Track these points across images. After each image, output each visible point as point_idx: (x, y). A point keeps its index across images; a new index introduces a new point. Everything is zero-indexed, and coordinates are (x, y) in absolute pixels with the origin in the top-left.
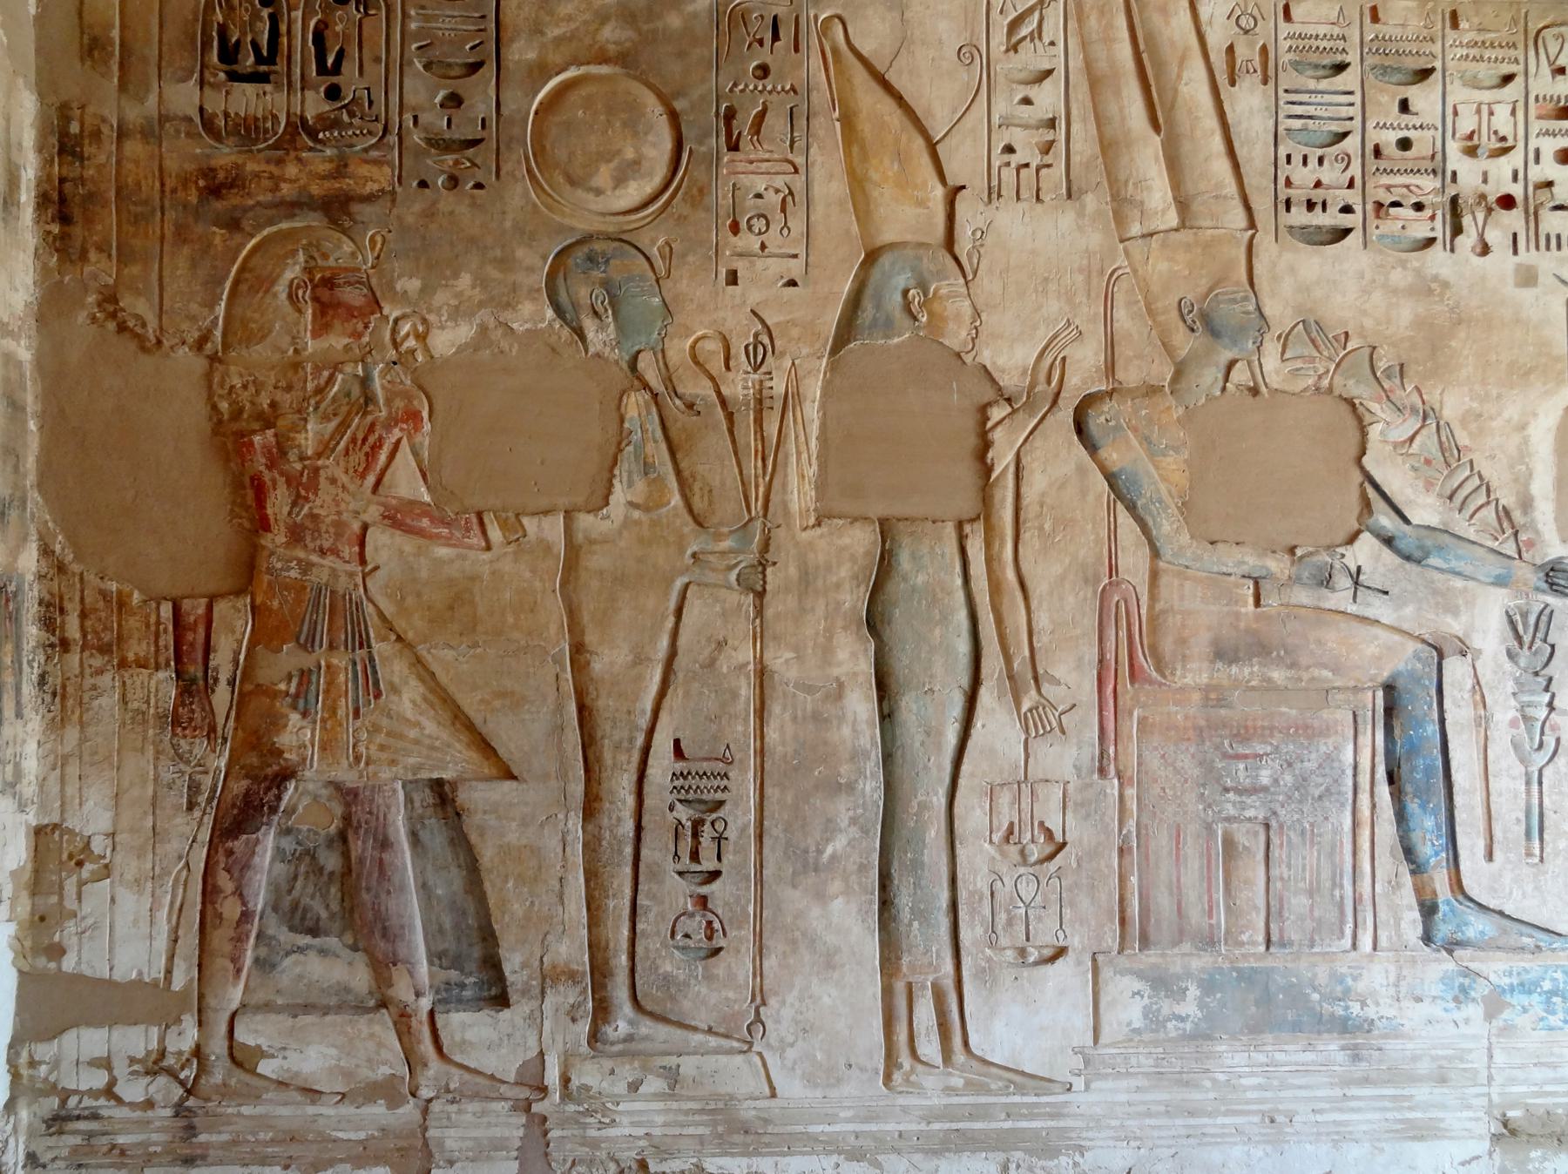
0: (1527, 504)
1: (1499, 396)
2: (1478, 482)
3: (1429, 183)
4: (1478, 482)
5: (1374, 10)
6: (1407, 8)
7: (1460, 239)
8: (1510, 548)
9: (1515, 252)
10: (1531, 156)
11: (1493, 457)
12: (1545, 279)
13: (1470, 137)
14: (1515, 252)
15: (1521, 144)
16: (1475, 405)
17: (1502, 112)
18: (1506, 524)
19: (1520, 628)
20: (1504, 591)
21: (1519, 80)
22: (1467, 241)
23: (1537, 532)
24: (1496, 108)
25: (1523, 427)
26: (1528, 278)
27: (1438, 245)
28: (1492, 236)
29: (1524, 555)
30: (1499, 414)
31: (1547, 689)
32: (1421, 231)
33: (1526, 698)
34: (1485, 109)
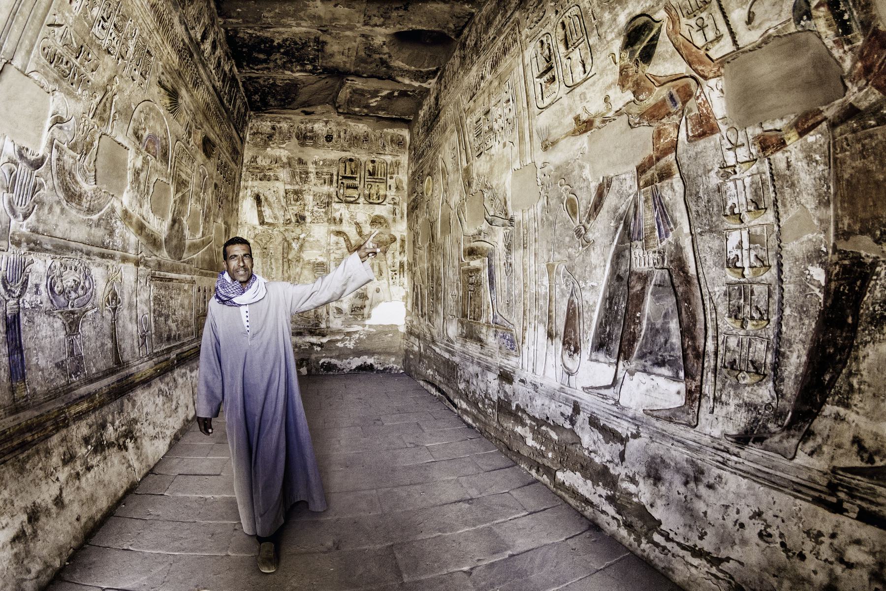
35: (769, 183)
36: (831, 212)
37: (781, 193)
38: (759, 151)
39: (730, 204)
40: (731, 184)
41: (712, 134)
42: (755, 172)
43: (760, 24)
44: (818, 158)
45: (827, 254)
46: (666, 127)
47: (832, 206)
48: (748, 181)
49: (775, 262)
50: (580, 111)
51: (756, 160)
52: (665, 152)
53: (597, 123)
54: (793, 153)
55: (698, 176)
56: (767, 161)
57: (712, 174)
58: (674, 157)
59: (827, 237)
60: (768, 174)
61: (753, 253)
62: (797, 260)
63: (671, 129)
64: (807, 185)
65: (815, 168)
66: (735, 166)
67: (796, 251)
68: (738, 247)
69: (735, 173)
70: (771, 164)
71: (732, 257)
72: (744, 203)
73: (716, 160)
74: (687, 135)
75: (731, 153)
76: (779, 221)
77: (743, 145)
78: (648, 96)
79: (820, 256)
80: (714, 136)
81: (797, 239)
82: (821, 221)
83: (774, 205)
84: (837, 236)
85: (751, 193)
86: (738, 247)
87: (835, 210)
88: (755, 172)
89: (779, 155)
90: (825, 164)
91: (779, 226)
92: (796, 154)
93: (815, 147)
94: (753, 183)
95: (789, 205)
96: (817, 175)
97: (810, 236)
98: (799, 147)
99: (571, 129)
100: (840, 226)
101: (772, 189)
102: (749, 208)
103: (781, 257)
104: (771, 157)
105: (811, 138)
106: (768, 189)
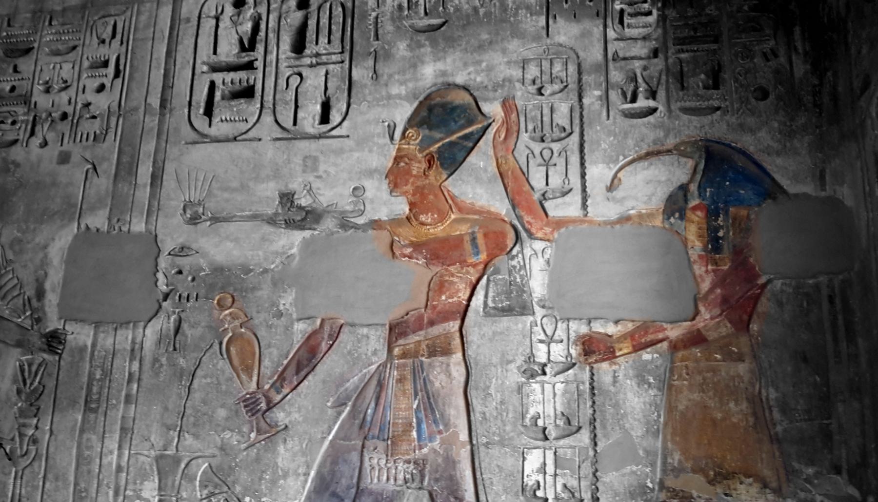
0: (40, 294)
1: (35, 230)
2: (16, 281)
3: (21, 110)
4: (16, 281)
5: (9, 20)
6: (26, 18)
7: (33, 138)
8: (27, 323)
9: (62, 145)
10: (81, 89)
11: (25, 266)
12: (75, 158)
13: (47, 82)
14: (62, 145)
15: (75, 84)
16: (19, 235)
17: (67, 67)
18: (27, 307)
19: (26, 374)
20: (19, 350)
21: (80, 49)
22: (36, 141)
23: (45, 313)
24: (64, 65)
25: (45, 247)
26: (64, 158)
27: (19, 144)
28: (50, 136)
29: (35, 327)
30: (33, 240)
31: (35, 416)
32: (10, 137)
33: (21, 421)
34: (58, 66)
35: (587, 395)
36: (659, 444)
37: (601, 411)
38: (580, 355)
39: (532, 412)
40: (536, 387)
41: (522, 314)
42: (571, 378)
43: (624, 198)
44: (652, 380)
45: (653, 490)
46: (455, 279)
47: (661, 436)
48: (560, 387)
49: (589, 496)
50: (295, 185)
51: (574, 364)
52: (445, 316)
53: (329, 223)
54: (623, 367)
55: (491, 364)
56: (588, 368)
57: (512, 367)
58: (457, 327)
59: (653, 471)
60: (587, 385)
61: (560, 482)
62: (616, 494)
63: (462, 286)
64: (634, 408)
65: (647, 391)
66: (545, 365)
67: (616, 484)
68: (538, 471)
69: (544, 373)
70: (593, 374)
71: (530, 483)
72: (552, 414)
73: (521, 350)
74: (485, 304)
75: (543, 348)
76: (596, 444)
77: (562, 341)
78: (434, 224)
79: (645, 493)
80: (524, 318)
81: (617, 470)
82: (647, 452)
83: (590, 424)
84: (664, 471)
85: (563, 404)
86: (538, 471)
87: (664, 442)
88: (571, 378)
89: (605, 365)
90: (659, 389)
91: (596, 451)
92: (625, 369)
93: (649, 367)
94: (566, 391)
95: (609, 428)
96: (647, 399)
97: (635, 468)
98: (631, 362)
99: (270, 212)
100: (670, 460)
101: (589, 403)
102: (558, 422)
103: (597, 489)
104: (595, 366)
105: (646, 356)
106: (585, 403)
